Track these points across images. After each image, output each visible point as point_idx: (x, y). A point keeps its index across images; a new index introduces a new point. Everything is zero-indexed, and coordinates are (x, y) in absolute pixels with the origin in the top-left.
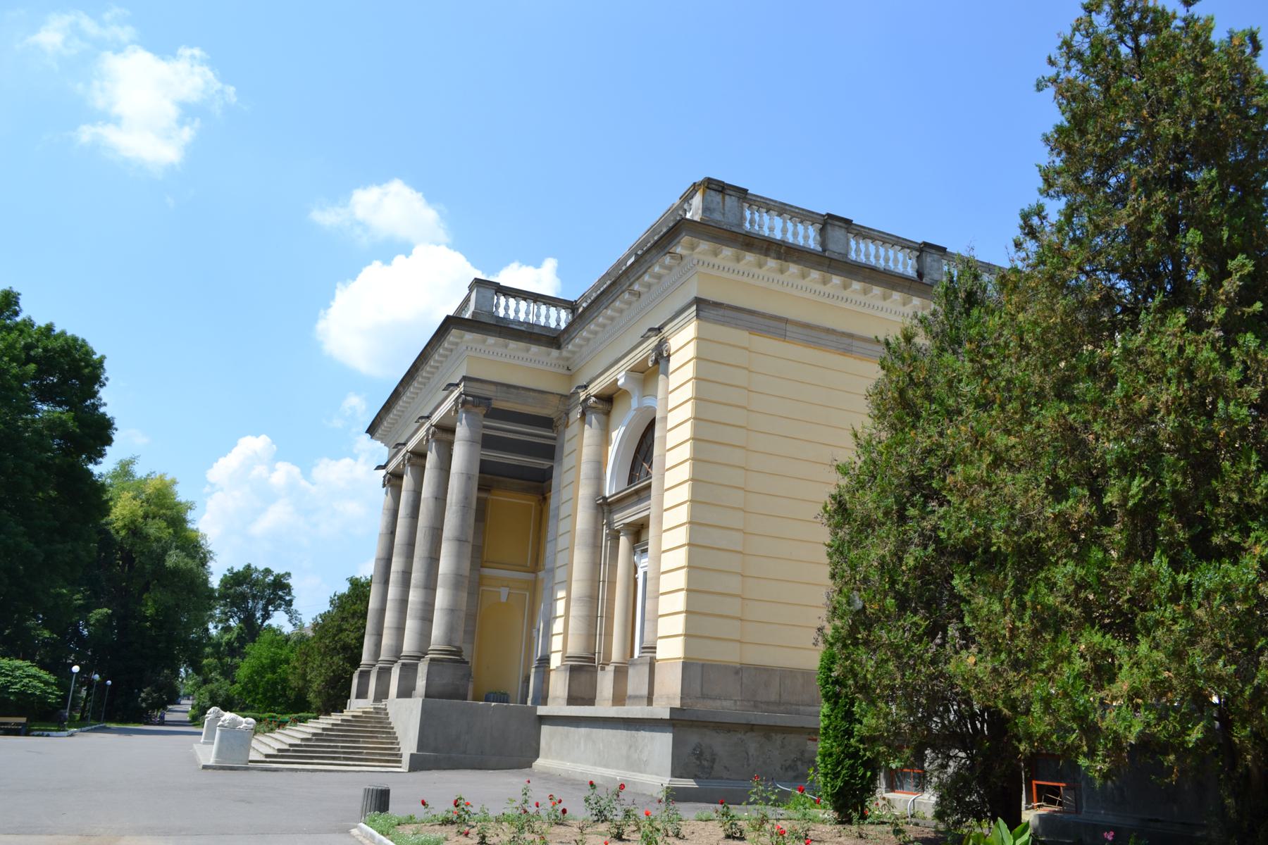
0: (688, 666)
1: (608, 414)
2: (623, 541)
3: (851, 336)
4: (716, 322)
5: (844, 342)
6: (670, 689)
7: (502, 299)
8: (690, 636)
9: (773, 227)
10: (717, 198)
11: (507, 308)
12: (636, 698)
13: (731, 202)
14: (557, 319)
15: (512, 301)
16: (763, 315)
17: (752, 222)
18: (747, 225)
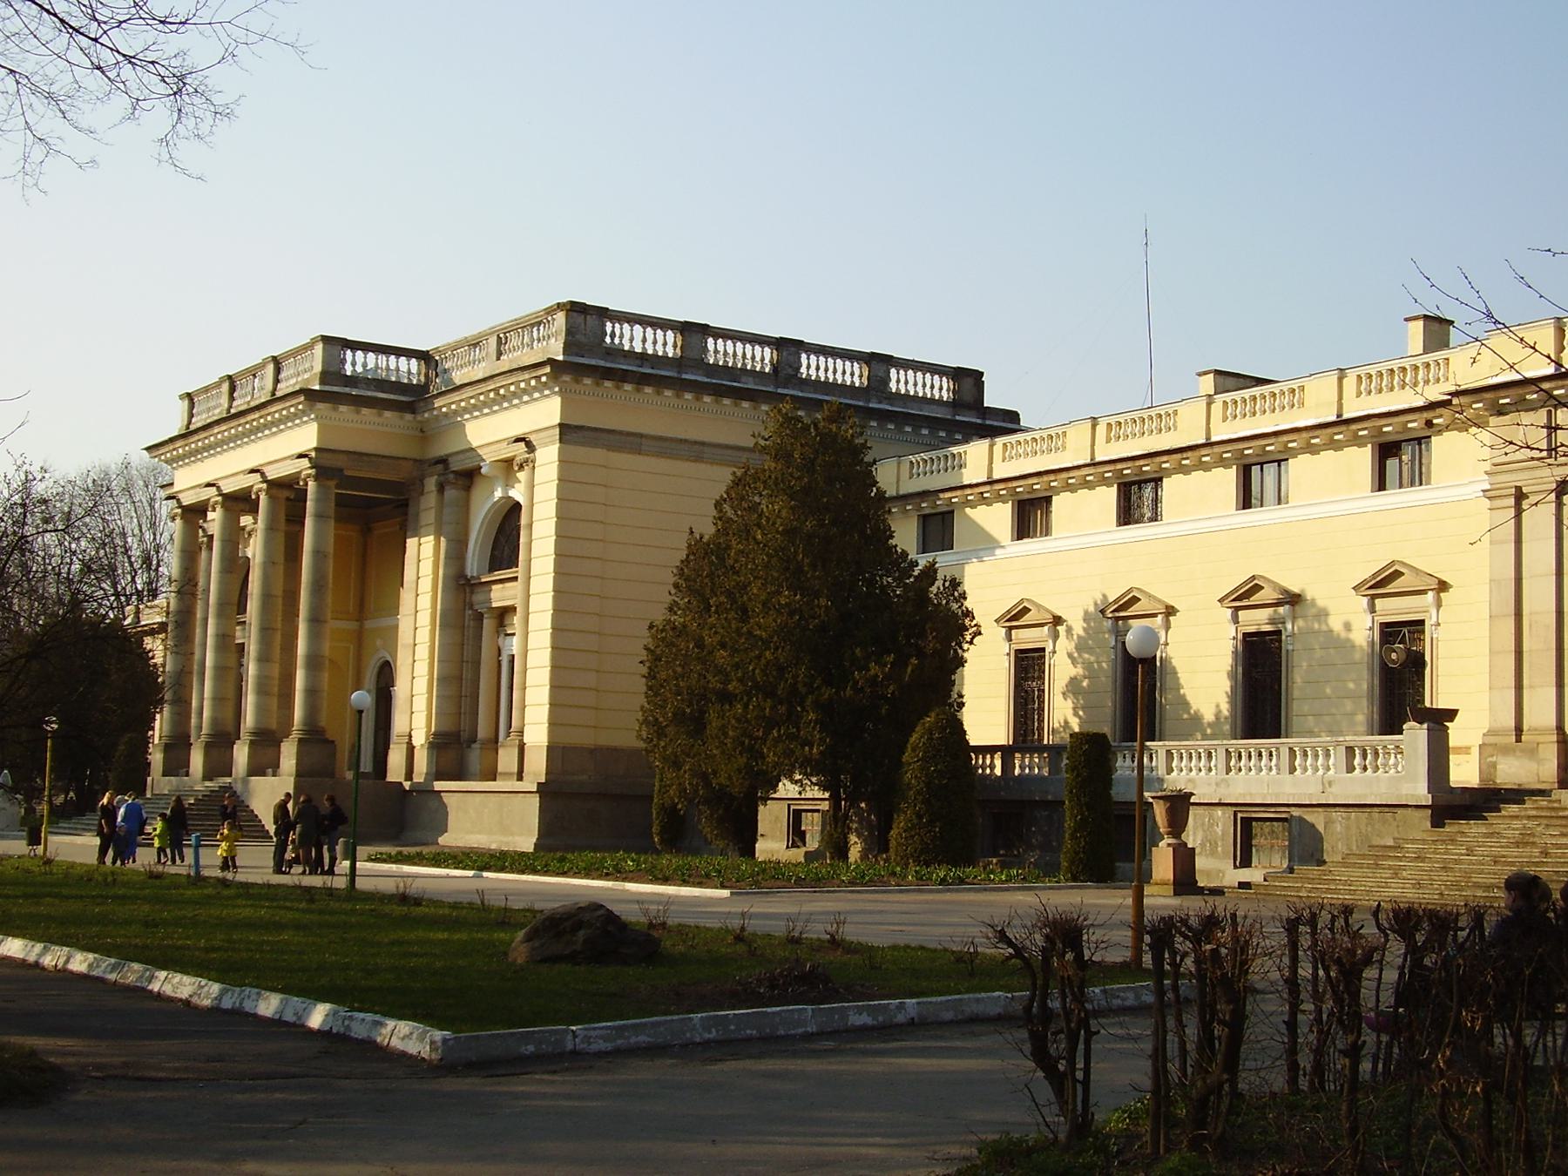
0: (551, 749)
1: (468, 488)
2: (488, 624)
3: (703, 444)
4: (576, 443)
5: (696, 451)
6: (537, 765)
7: (349, 353)
8: (553, 724)
9: (633, 339)
10: (580, 319)
11: (354, 364)
12: (507, 775)
13: (592, 320)
14: (409, 369)
15: (359, 353)
16: (621, 433)
17: (613, 335)
18: (608, 340)
